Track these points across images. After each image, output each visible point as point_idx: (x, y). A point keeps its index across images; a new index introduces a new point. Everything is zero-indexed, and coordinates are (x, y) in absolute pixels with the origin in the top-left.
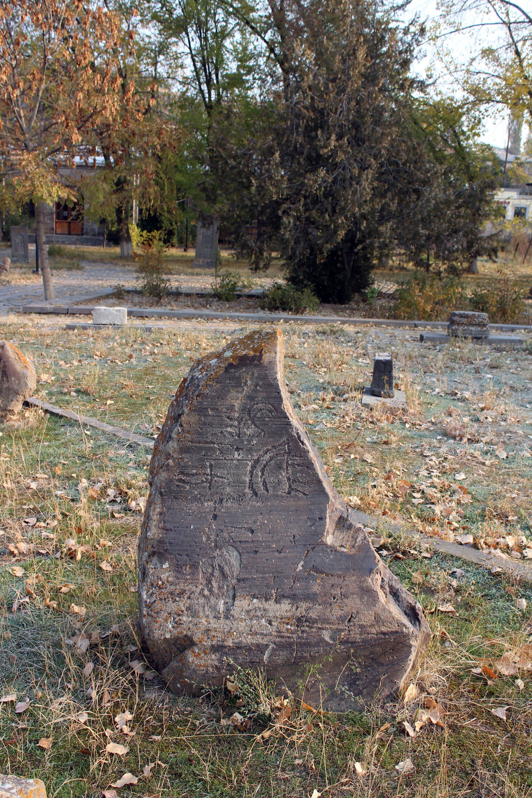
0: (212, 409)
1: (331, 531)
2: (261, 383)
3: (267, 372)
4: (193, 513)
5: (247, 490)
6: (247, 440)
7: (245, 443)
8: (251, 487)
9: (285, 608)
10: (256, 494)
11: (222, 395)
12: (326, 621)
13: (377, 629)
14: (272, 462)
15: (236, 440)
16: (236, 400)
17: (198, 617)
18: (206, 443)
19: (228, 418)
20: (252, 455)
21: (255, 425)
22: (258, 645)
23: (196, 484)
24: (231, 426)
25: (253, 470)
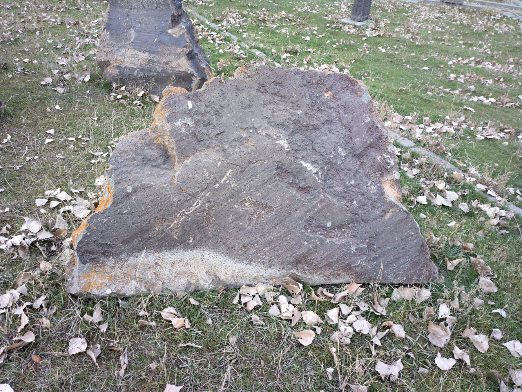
5: (141, 5)
8: (142, 4)
9: (146, 55)
10: (144, 7)
12: (159, 62)
22: (132, 68)
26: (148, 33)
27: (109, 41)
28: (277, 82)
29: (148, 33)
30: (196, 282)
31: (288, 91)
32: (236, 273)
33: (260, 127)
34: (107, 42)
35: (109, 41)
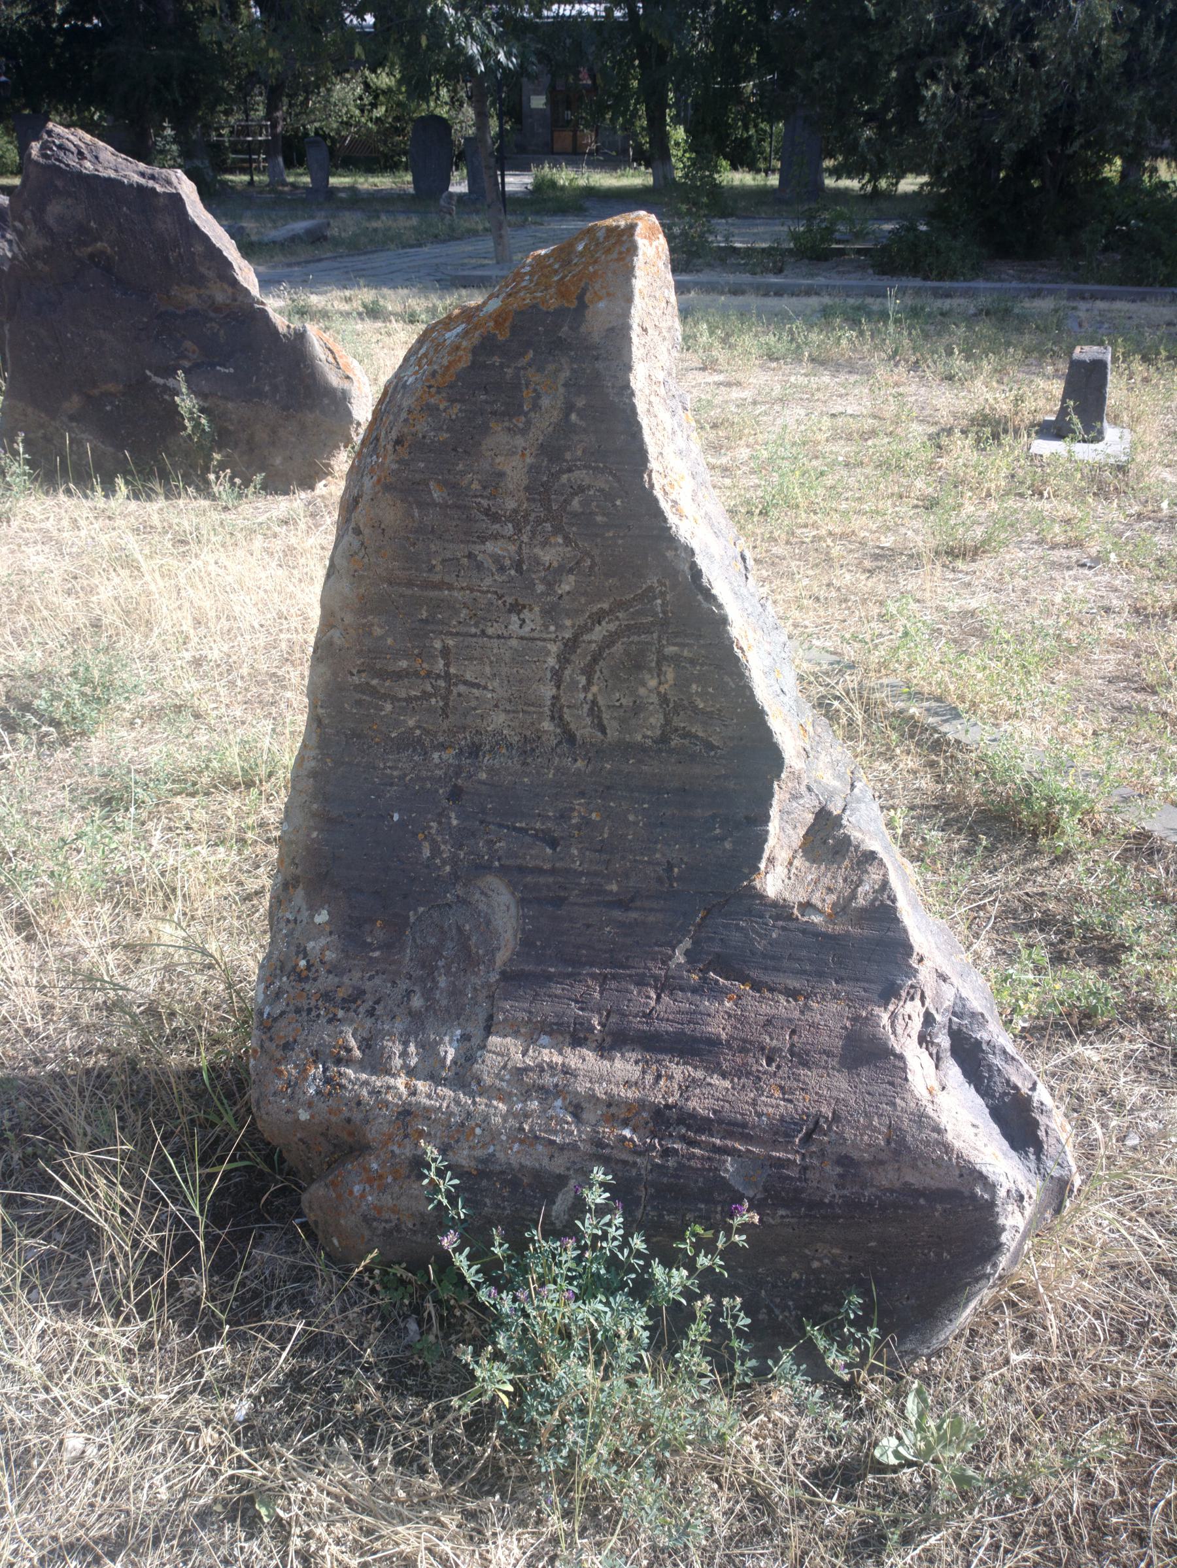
0: (444, 484)
1: (783, 855)
2: (580, 403)
3: (599, 365)
4: (402, 778)
5: (547, 725)
6: (543, 580)
7: (540, 588)
8: (557, 716)
10: (570, 738)
11: (465, 440)
13: (892, 1175)
14: (618, 648)
15: (511, 580)
16: (511, 457)
17: (388, 1072)
18: (428, 585)
19: (487, 512)
20: (560, 627)
21: (566, 538)
22: (537, 1175)
23: (409, 700)
24: (496, 537)
25: (562, 669)
26: (622, 903)
29: (622, 903)
34: (326, 981)
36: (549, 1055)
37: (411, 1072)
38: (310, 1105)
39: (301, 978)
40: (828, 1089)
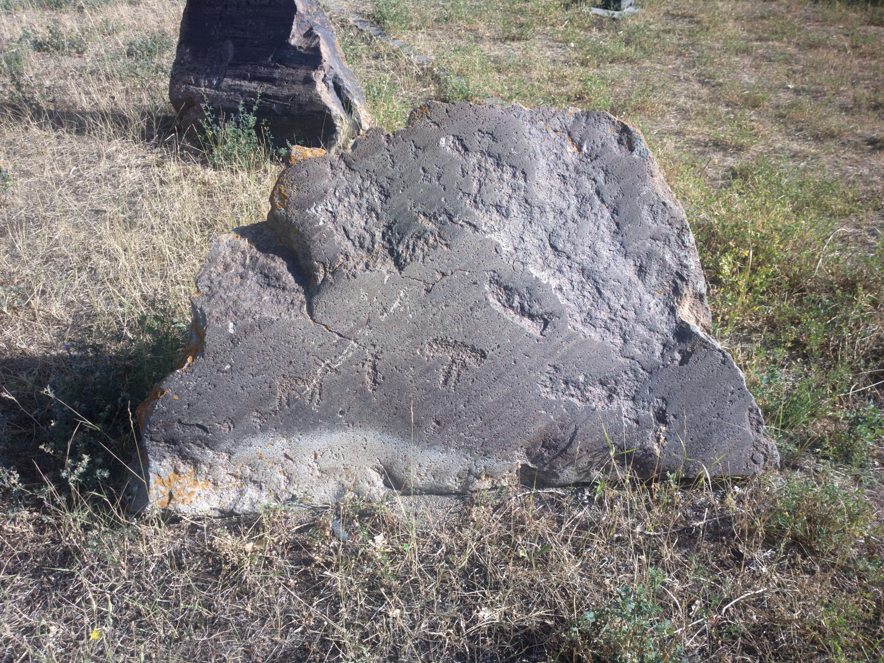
27: (190, 63)
28: (484, 131)
30: (354, 485)
31: (505, 146)
32: (424, 469)
33: (456, 213)
34: (188, 66)
35: (190, 63)
36: (238, 82)
37: (206, 87)
38: (182, 94)
39: (182, 65)
40: (298, 89)
